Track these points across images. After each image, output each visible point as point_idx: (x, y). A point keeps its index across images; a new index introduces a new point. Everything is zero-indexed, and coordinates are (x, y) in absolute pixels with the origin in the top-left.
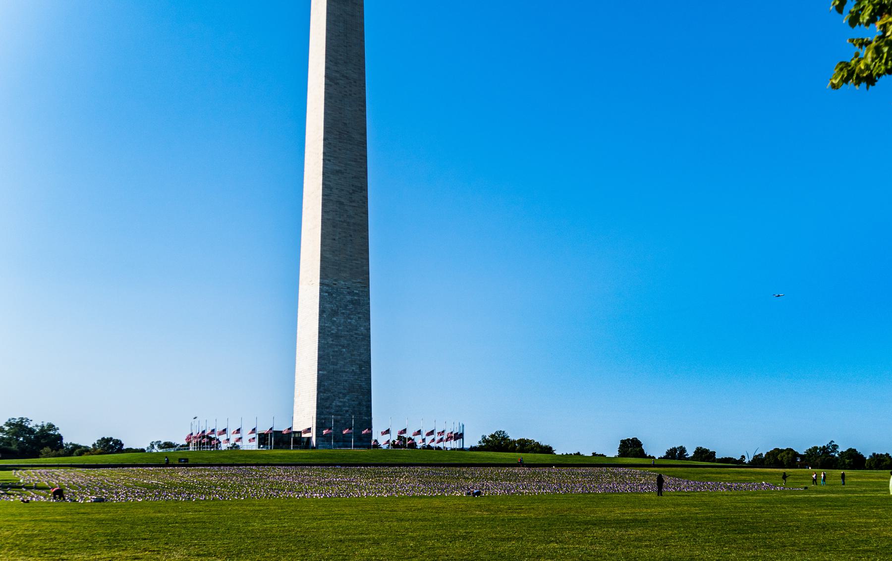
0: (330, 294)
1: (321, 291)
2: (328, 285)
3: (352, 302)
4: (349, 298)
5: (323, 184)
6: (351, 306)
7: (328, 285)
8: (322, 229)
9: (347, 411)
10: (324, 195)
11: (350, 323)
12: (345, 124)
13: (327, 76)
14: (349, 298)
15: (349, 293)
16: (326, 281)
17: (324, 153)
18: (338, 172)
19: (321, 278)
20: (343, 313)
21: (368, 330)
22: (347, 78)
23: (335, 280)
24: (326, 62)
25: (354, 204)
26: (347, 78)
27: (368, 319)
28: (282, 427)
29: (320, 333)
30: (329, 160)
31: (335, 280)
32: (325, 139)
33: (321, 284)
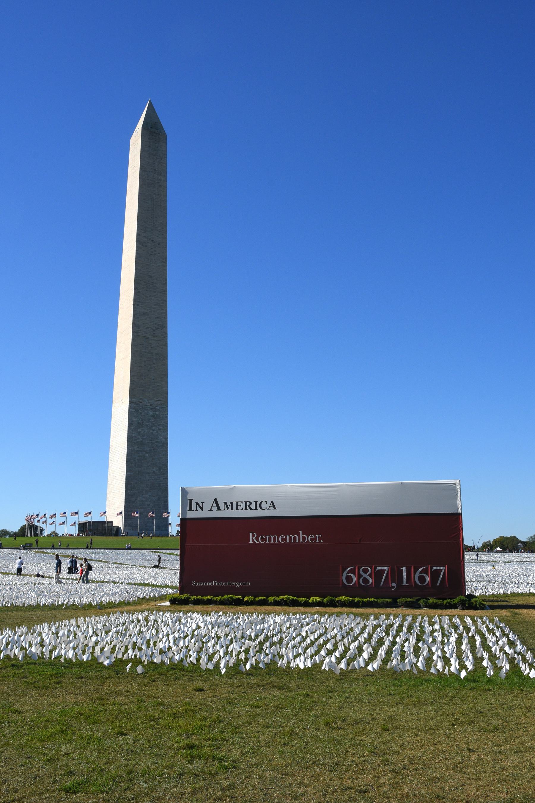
0: (137, 410)
2: (135, 403)
4: (151, 413)
5: (133, 323)
7: (135, 403)
8: (131, 359)
9: (149, 505)
10: (133, 332)
11: (152, 433)
12: (151, 277)
13: (138, 241)
14: (151, 413)
15: (151, 409)
16: (134, 400)
17: (135, 300)
18: (145, 314)
19: (130, 398)
20: (147, 425)
21: (166, 438)
22: (153, 242)
23: (141, 399)
24: (137, 230)
25: (156, 339)
26: (153, 242)
27: (167, 430)
28: (96, 517)
29: (128, 441)
30: (138, 305)
31: (141, 399)
32: (135, 289)
33: (130, 402)
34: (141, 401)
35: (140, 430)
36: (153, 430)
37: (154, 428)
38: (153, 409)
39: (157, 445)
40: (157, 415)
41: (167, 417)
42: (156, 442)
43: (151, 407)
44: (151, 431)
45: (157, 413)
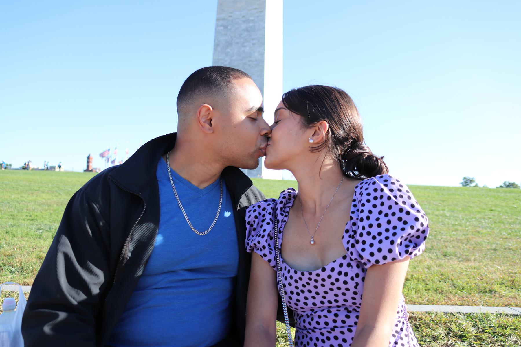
0: (225, 27)
1: (217, 26)
3: (247, 30)
4: (243, 26)
6: (245, 34)
7: (224, 19)
15: (244, 22)
20: (237, 43)
21: (262, 54)
23: (231, 13)
31: (231, 13)
34: (230, 15)
35: (228, 50)
36: (245, 47)
37: (246, 44)
38: (247, 21)
39: (249, 65)
40: (251, 27)
41: (264, 28)
42: (249, 61)
43: (244, 19)
44: (243, 49)
45: (251, 24)
